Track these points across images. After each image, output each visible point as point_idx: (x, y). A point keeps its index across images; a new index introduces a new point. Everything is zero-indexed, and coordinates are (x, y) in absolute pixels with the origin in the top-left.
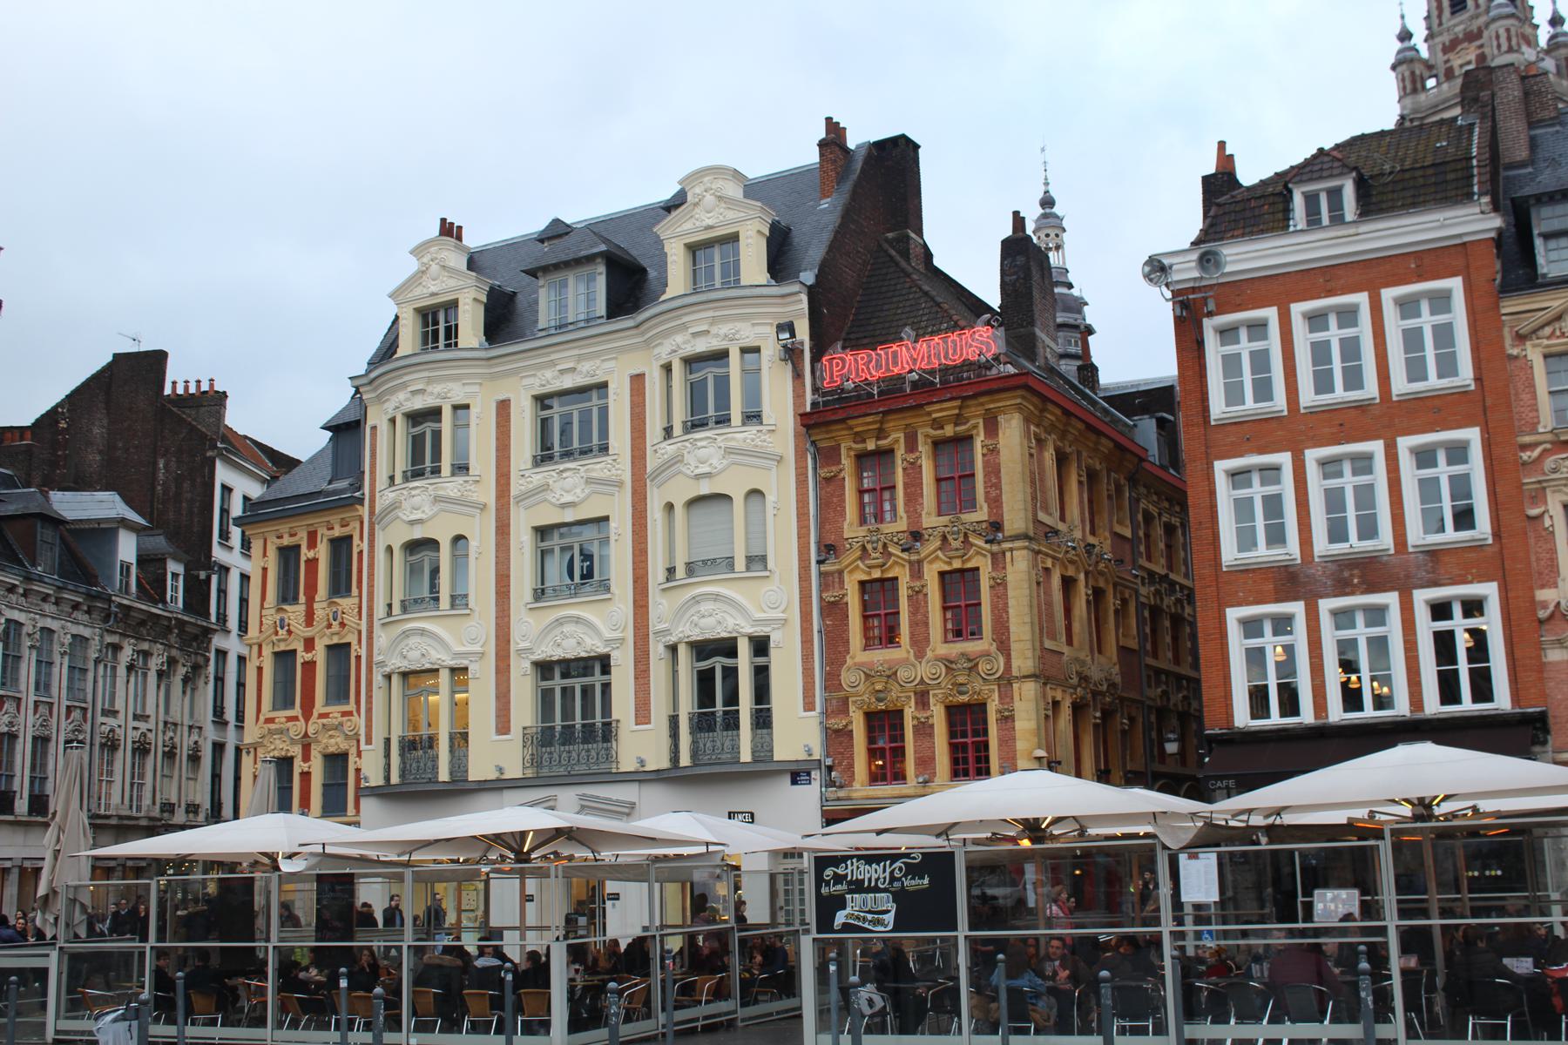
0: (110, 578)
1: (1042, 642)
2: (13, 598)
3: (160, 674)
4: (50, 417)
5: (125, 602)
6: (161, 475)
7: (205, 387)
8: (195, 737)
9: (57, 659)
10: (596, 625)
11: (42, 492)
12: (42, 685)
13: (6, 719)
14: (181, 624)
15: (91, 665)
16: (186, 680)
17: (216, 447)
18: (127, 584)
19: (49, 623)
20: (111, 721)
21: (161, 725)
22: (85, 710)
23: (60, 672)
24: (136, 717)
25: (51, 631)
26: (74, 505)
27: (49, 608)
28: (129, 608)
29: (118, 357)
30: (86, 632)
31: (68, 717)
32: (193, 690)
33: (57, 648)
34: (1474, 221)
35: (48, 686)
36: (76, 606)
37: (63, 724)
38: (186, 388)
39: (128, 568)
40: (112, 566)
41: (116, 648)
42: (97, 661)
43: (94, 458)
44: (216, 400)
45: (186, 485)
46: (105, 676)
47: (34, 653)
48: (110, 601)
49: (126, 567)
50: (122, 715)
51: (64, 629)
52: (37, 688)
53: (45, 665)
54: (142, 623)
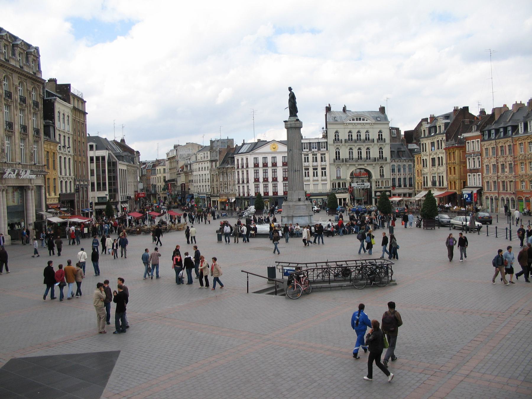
1: (460, 174)
23: (407, 169)
34: (478, 133)
51: (407, 164)
53: (404, 169)
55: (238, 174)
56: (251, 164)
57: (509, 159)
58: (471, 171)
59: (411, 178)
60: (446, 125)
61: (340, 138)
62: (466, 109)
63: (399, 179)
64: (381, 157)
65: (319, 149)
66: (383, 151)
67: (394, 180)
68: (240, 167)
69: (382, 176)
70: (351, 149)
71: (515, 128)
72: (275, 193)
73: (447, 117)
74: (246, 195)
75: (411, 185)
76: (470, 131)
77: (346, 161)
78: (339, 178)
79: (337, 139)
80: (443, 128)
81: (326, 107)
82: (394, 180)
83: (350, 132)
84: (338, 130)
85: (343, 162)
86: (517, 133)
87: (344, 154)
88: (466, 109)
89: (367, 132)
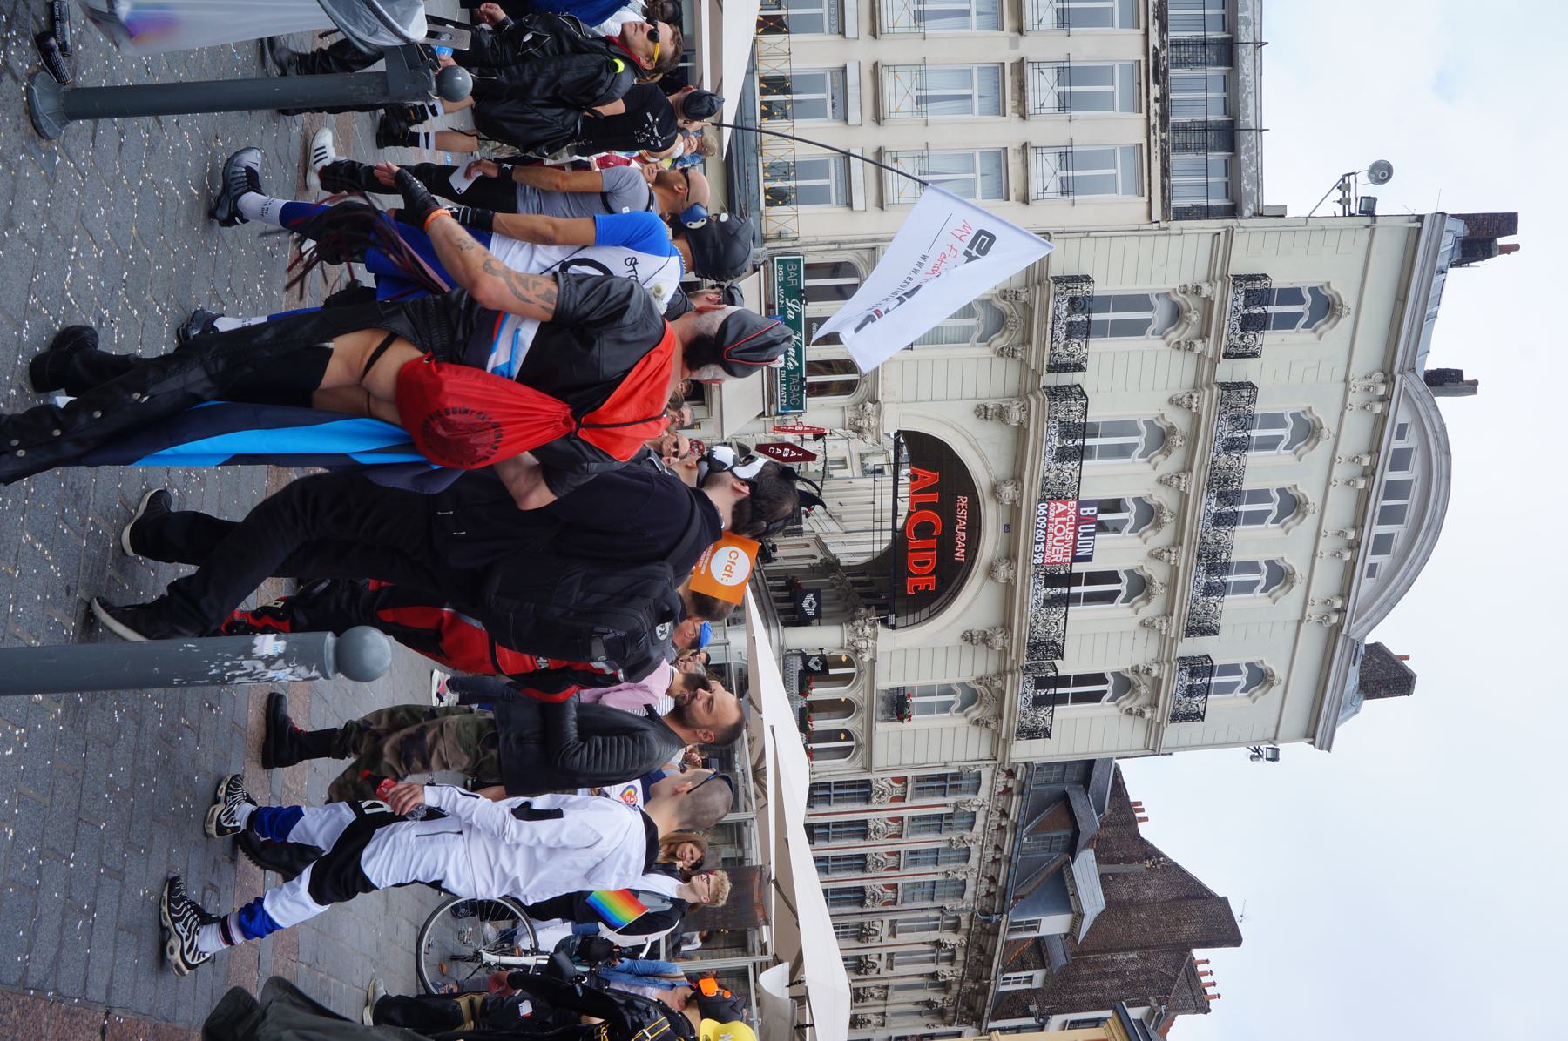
0: (1023, 912)
2: (996, 817)
3: (934, 976)
4: (1151, 853)
5: (1002, 929)
6: (1120, 957)
7: (1210, 991)
8: (874, 1020)
9: (941, 868)
11: (1092, 840)
12: (915, 857)
13: (881, 826)
14: (984, 991)
15: (938, 903)
16: (929, 1003)
17: (1160, 1004)
18: (1020, 930)
19: (975, 855)
20: (885, 932)
21: (885, 983)
22: (895, 903)
23: (928, 873)
24: (890, 955)
25: (967, 859)
26: (1085, 868)
27: (989, 853)
28: (997, 934)
29: (1224, 901)
30: (968, 895)
31: (887, 886)
32: (919, 1013)
33: (951, 867)
35: (915, 862)
36: (993, 880)
37: (880, 883)
38: (1205, 974)
39: (1034, 929)
40: (1035, 911)
41: (956, 928)
42: (942, 909)
43: (1124, 892)
44: (1199, 1003)
45: (1117, 982)
46: (928, 919)
47: (945, 845)
48: (1001, 913)
49: (1033, 926)
50: (892, 941)
51: (969, 872)
52: (912, 853)
53: (935, 857)
54: (982, 950)
59: (862, 903)
61: (1270, 339)
63: (861, 830)
64: (1051, 690)
66: (1104, 708)
70: (1161, 439)
77: (1060, 394)
79: (1260, 306)
81: (1508, 223)
83: (1307, 431)
84: (1345, 323)
85: (1055, 368)
89: (1279, 576)
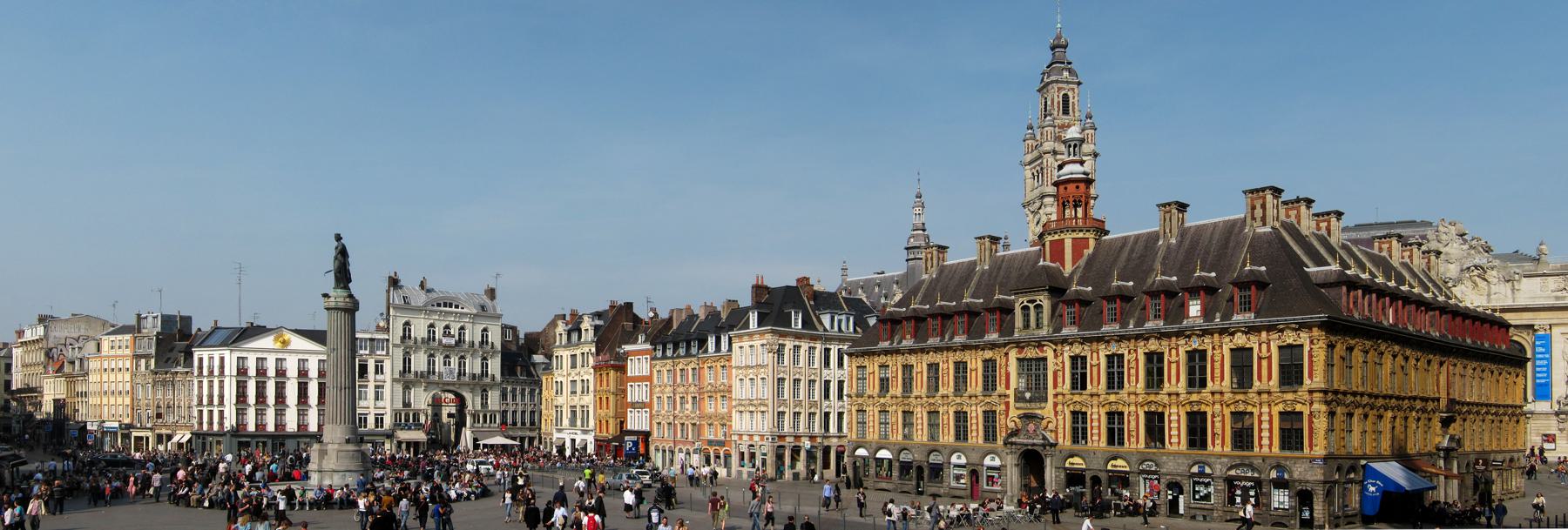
10: (576, 400)
55: (200, 387)
56: (231, 368)
57: (692, 389)
58: (634, 405)
60: (597, 328)
62: (629, 305)
65: (372, 352)
67: (504, 413)
68: (205, 372)
69: (485, 405)
71: (702, 343)
72: (280, 425)
73: (598, 315)
74: (216, 427)
75: (532, 423)
76: (635, 342)
78: (406, 405)
80: (591, 333)
82: (504, 413)
83: (432, 326)
86: (706, 351)
87: (419, 362)
88: (629, 305)
